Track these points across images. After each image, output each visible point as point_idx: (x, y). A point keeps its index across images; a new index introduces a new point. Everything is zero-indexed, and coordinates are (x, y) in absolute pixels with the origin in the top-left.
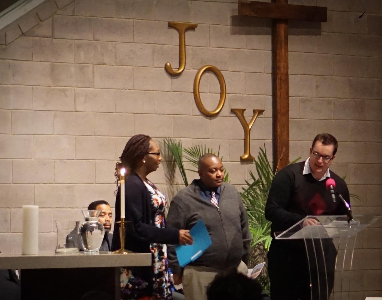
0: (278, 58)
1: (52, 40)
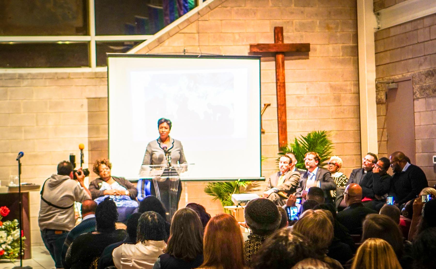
0: (278, 74)
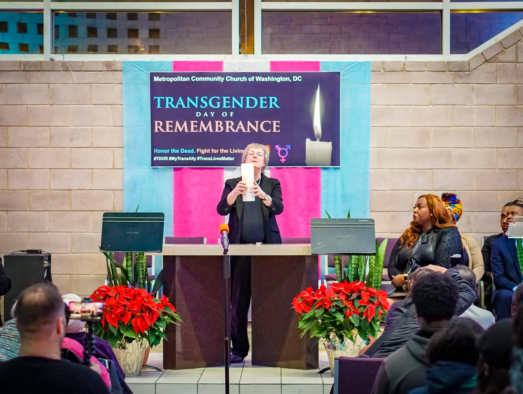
1: (516, 65)
